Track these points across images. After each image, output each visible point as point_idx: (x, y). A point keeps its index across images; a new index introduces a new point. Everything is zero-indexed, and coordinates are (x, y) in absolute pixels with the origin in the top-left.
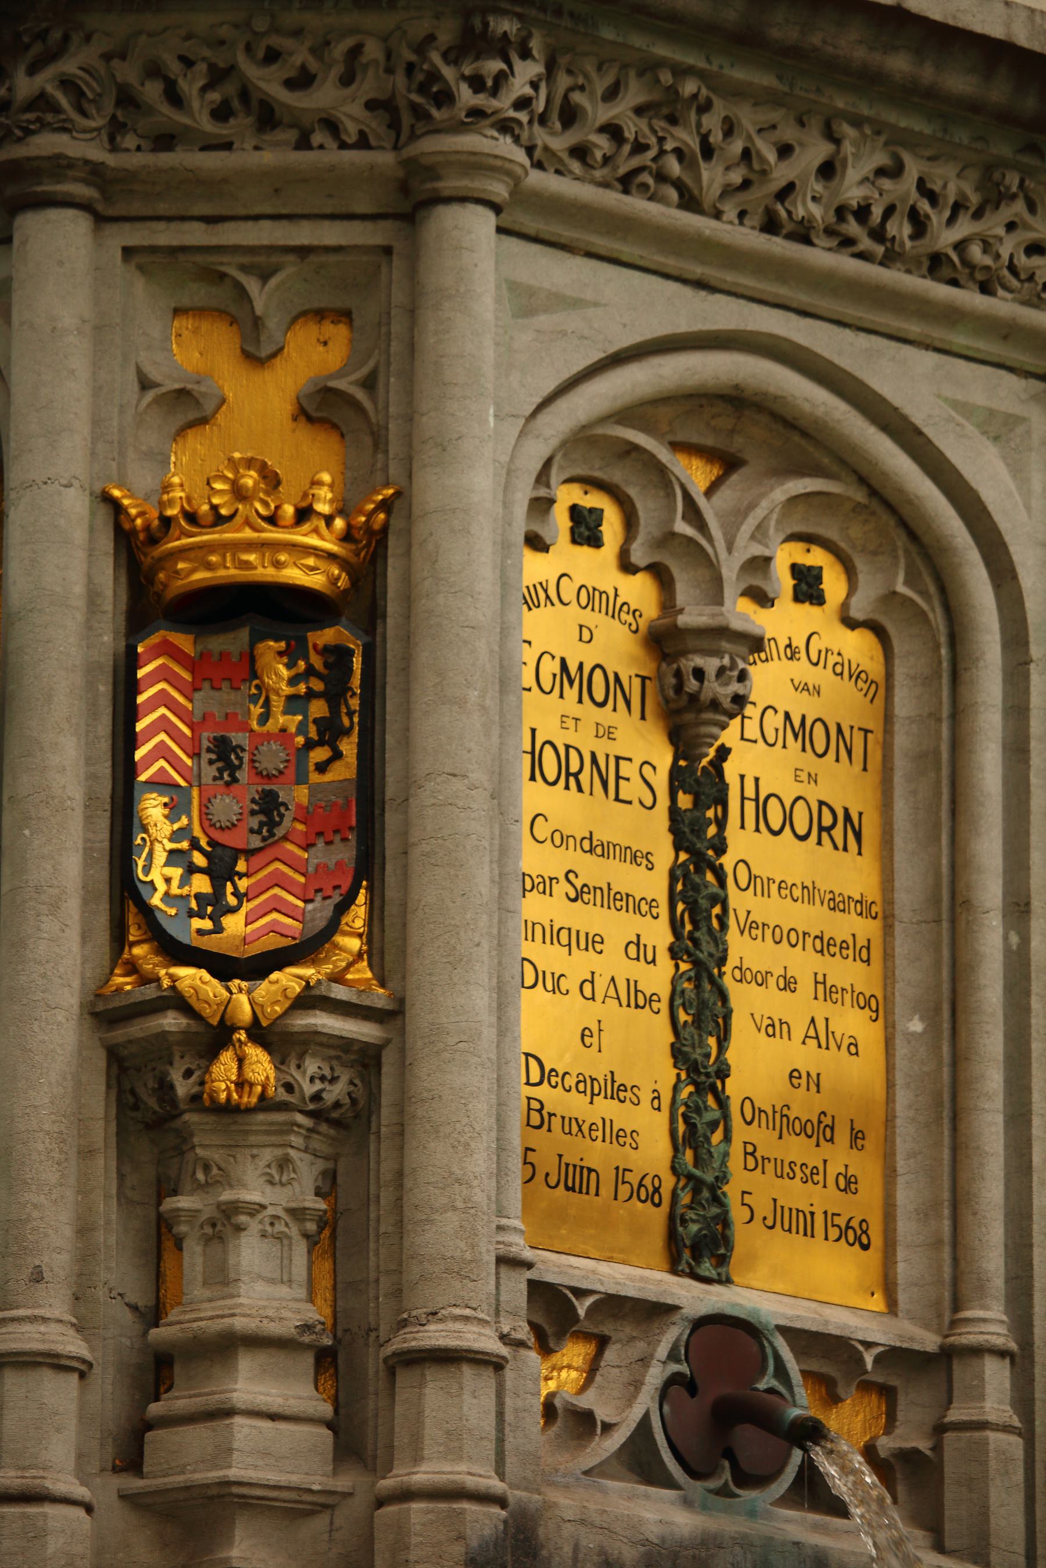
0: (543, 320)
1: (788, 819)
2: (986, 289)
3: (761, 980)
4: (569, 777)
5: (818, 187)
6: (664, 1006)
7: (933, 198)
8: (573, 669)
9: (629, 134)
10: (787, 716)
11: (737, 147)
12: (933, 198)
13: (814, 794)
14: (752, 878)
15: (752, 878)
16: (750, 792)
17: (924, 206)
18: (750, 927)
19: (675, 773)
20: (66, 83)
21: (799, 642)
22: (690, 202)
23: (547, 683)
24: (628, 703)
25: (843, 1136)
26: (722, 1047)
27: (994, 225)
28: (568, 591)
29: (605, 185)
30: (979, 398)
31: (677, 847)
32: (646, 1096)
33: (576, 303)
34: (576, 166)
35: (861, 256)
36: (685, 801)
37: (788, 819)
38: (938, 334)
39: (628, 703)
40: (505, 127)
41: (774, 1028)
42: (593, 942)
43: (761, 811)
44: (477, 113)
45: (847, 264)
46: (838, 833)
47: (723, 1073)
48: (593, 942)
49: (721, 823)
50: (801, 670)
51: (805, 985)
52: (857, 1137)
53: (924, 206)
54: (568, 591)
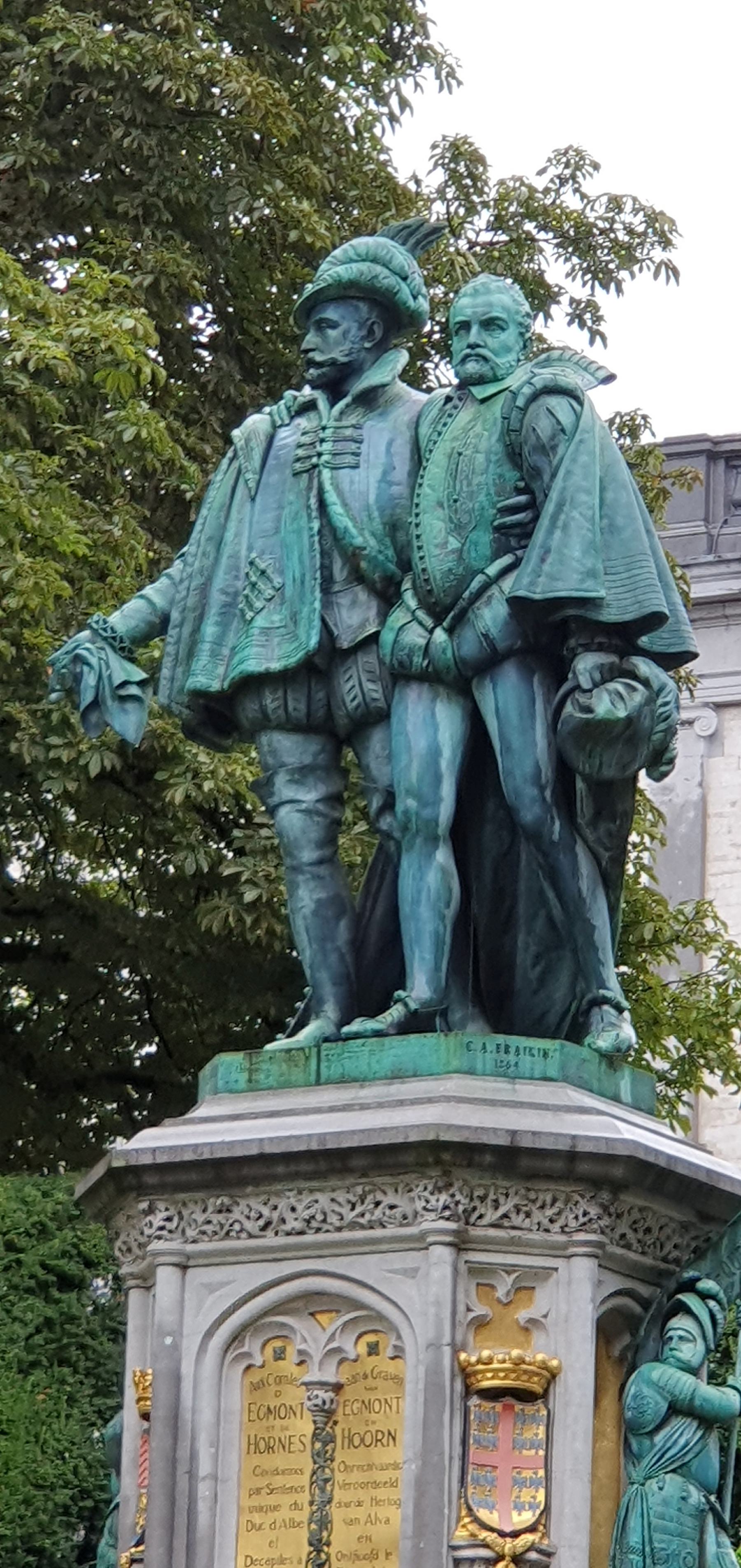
0: (218, 1293)
1: (362, 1440)
2: (384, 1227)
3: (347, 1505)
4: (269, 1448)
5: (294, 1215)
6: (306, 1524)
7: (340, 1204)
8: (272, 1408)
9: (215, 1222)
10: (363, 1402)
11: (253, 1214)
12: (340, 1204)
13: (373, 1429)
14: (346, 1467)
15: (346, 1467)
16: (346, 1435)
17: (337, 1208)
18: (345, 1486)
19: (314, 1435)
20: (120, 1249)
21: (368, 1372)
22: (251, 1236)
23: (261, 1416)
24: (295, 1414)
25: (382, 1556)
26: (329, 1536)
27: (369, 1204)
28: (271, 1380)
29: (222, 1240)
30: (397, 1266)
31: (315, 1463)
32: (295, 1561)
33: (228, 1283)
34: (206, 1238)
35: (327, 1231)
36: (318, 1445)
37: (362, 1440)
38: (374, 1248)
39: (295, 1414)
40: (159, 1238)
41: (351, 1522)
42: (276, 1508)
43: (351, 1441)
44: (149, 1237)
45: (321, 1237)
46: (385, 1441)
47: (328, 1544)
48: (276, 1508)
49: (334, 1450)
50: (370, 1382)
51: (367, 1503)
52: (388, 1554)
53: (337, 1208)
54: (271, 1380)
